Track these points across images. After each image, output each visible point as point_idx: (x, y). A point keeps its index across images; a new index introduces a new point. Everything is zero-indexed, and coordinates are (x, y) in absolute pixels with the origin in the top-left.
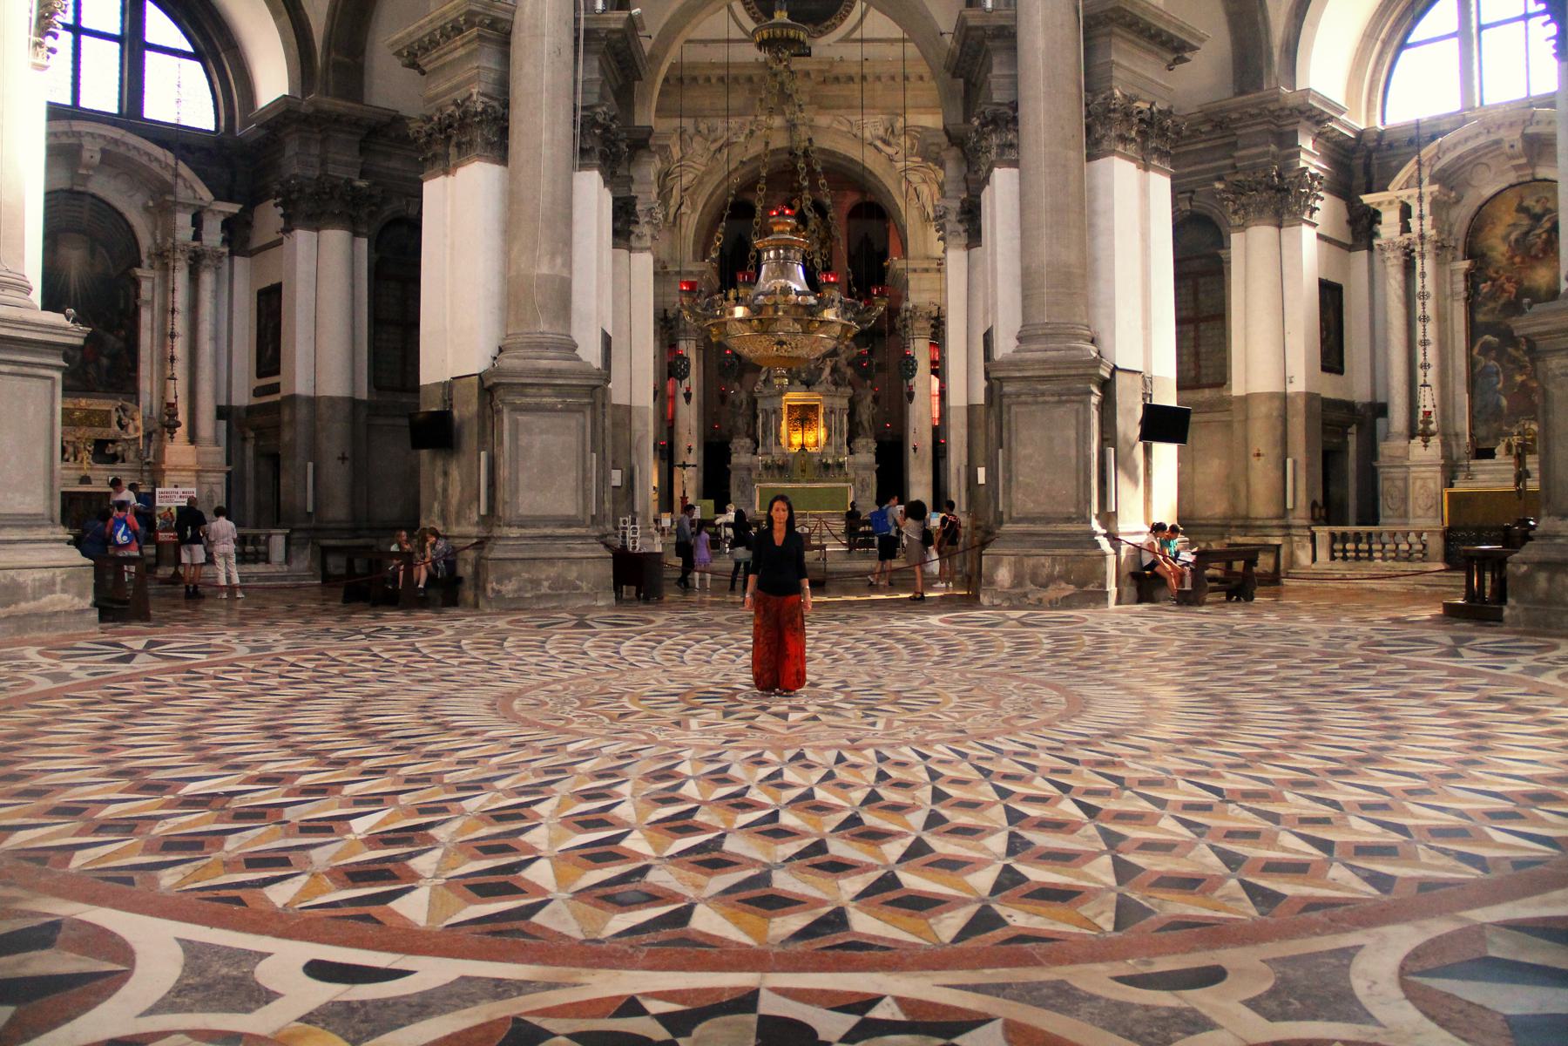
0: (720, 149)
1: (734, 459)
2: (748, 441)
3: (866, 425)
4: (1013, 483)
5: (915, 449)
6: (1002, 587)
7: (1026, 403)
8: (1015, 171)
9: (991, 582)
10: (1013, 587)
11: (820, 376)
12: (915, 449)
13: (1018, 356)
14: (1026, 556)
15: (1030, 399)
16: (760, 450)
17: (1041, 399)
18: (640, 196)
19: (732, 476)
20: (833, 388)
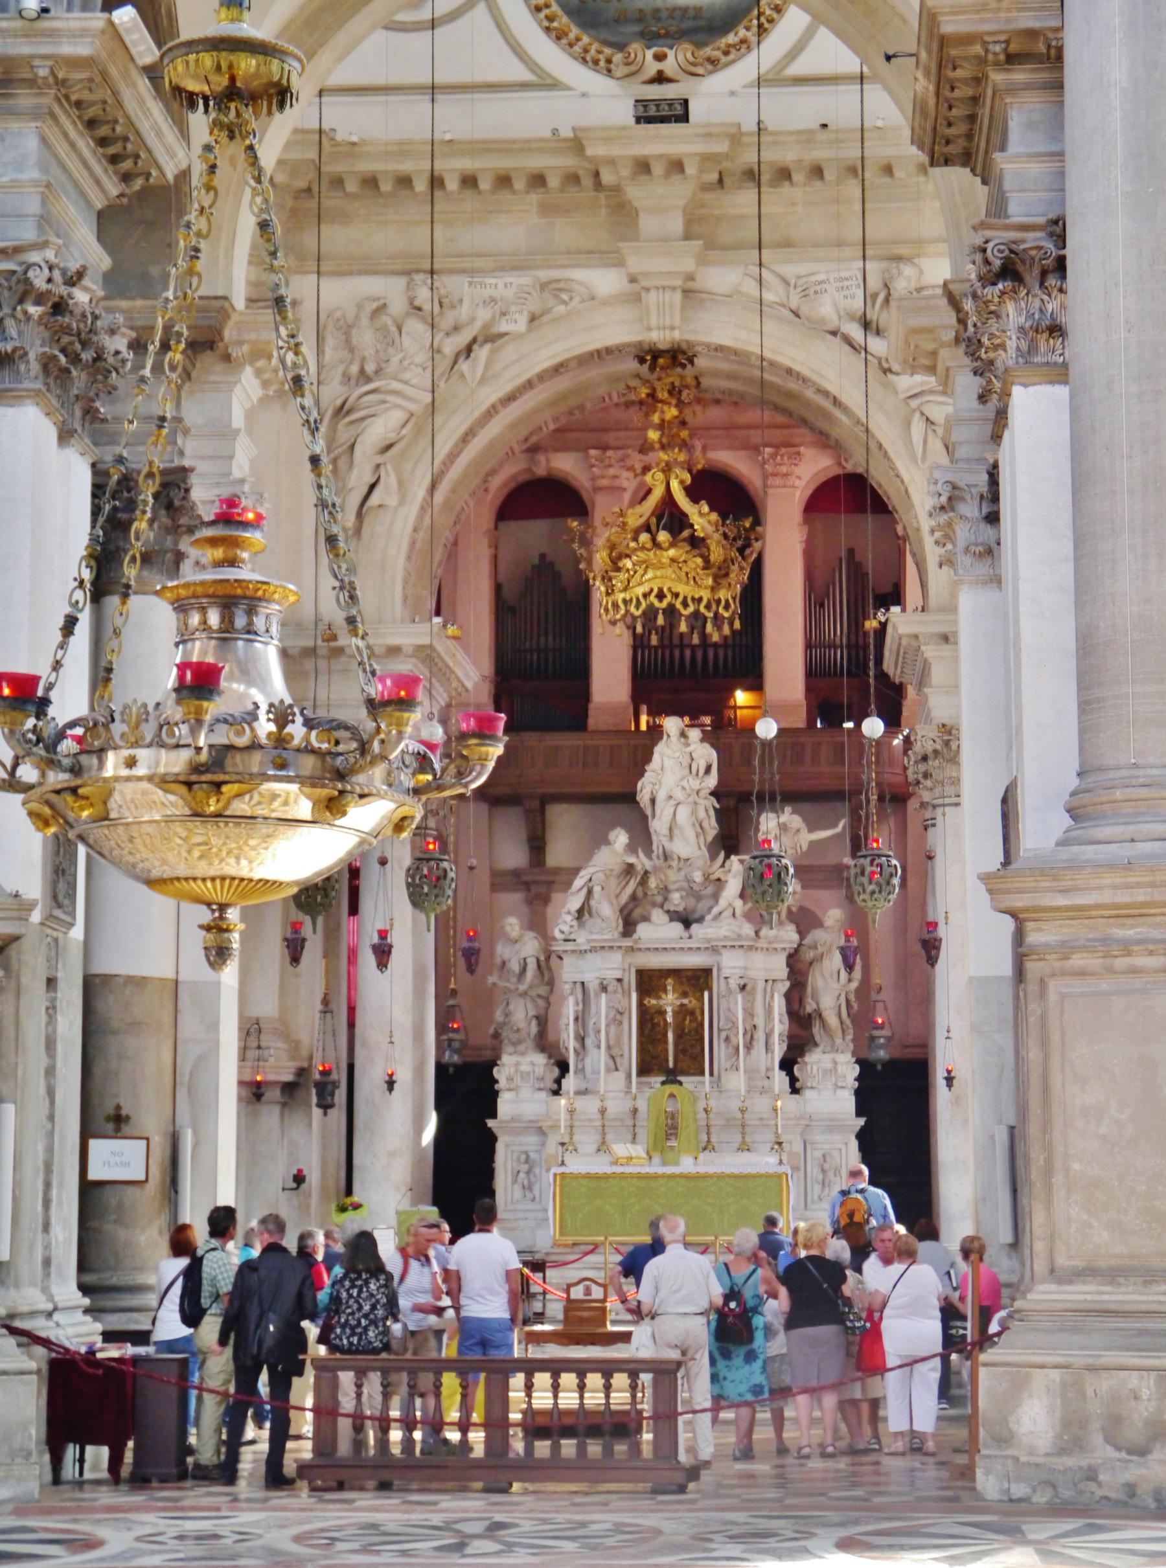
0: (469, 350)
1: (506, 1105)
2: (540, 1060)
3: (832, 1020)
4: (1058, 1179)
5: (949, 1080)
6: (1032, 1451)
7: (1082, 973)
8: (1061, 392)
9: (1005, 1439)
10: (1062, 1451)
11: (716, 897)
12: (949, 1080)
13: (1065, 853)
14: (1092, 1369)
15: (1093, 962)
16: (570, 1083)
17: (1121, 963)
18: (202, 467)
19: (500, 1147)
20: (748, 929)
